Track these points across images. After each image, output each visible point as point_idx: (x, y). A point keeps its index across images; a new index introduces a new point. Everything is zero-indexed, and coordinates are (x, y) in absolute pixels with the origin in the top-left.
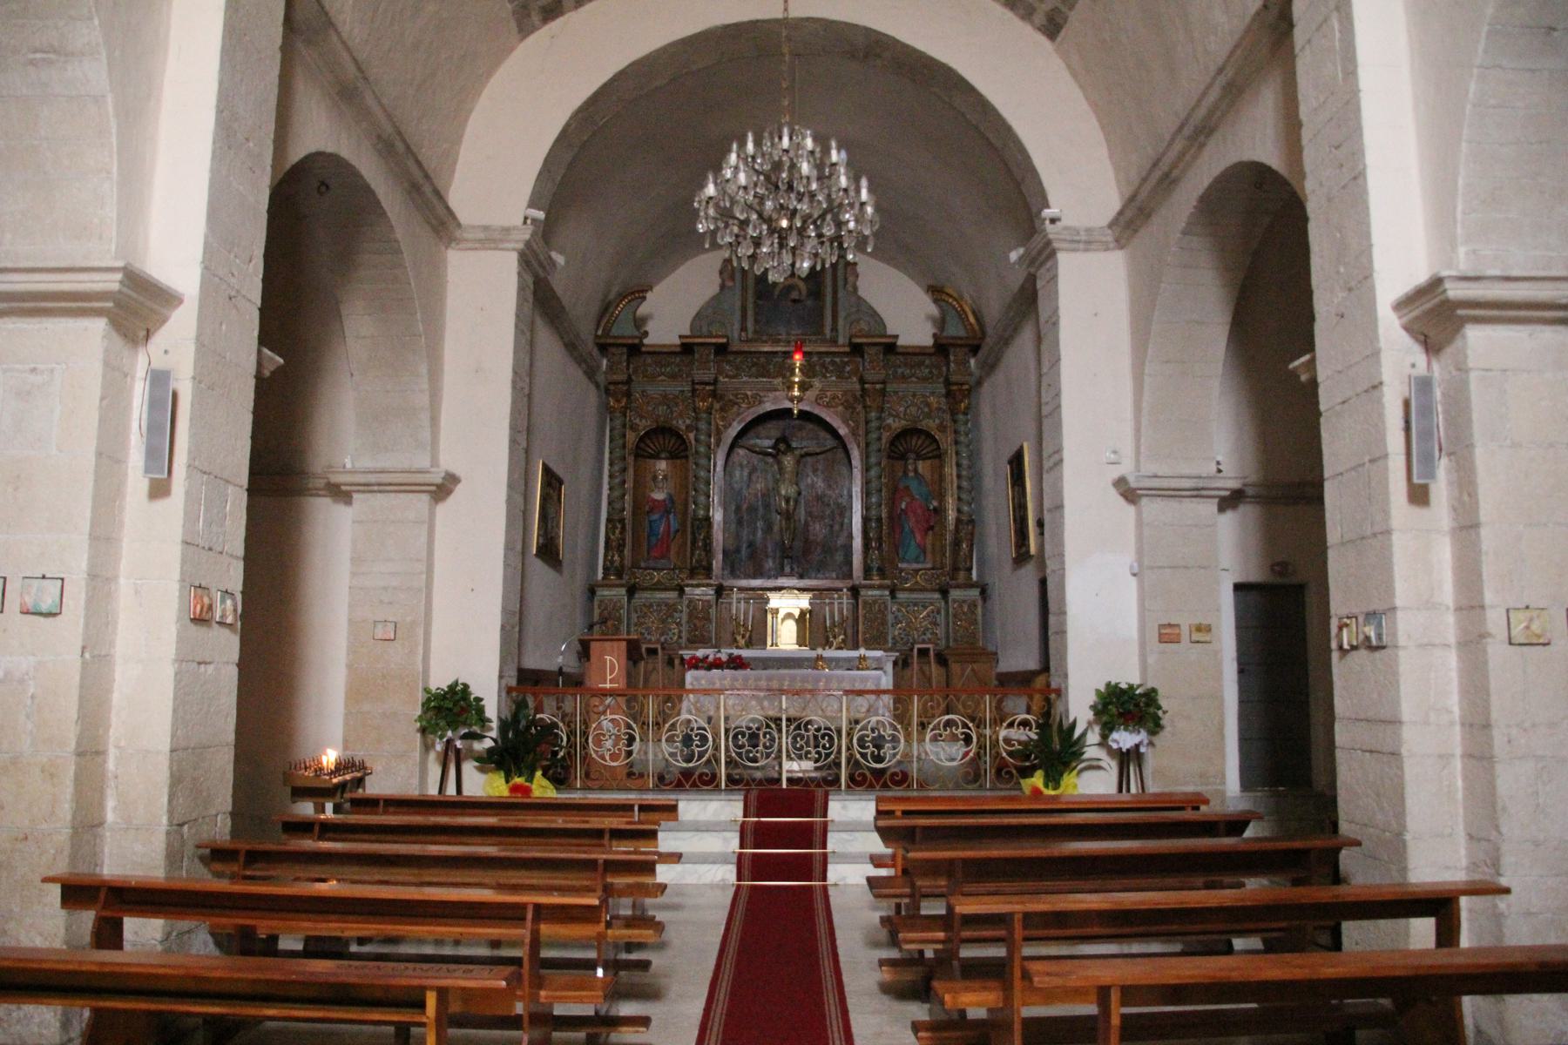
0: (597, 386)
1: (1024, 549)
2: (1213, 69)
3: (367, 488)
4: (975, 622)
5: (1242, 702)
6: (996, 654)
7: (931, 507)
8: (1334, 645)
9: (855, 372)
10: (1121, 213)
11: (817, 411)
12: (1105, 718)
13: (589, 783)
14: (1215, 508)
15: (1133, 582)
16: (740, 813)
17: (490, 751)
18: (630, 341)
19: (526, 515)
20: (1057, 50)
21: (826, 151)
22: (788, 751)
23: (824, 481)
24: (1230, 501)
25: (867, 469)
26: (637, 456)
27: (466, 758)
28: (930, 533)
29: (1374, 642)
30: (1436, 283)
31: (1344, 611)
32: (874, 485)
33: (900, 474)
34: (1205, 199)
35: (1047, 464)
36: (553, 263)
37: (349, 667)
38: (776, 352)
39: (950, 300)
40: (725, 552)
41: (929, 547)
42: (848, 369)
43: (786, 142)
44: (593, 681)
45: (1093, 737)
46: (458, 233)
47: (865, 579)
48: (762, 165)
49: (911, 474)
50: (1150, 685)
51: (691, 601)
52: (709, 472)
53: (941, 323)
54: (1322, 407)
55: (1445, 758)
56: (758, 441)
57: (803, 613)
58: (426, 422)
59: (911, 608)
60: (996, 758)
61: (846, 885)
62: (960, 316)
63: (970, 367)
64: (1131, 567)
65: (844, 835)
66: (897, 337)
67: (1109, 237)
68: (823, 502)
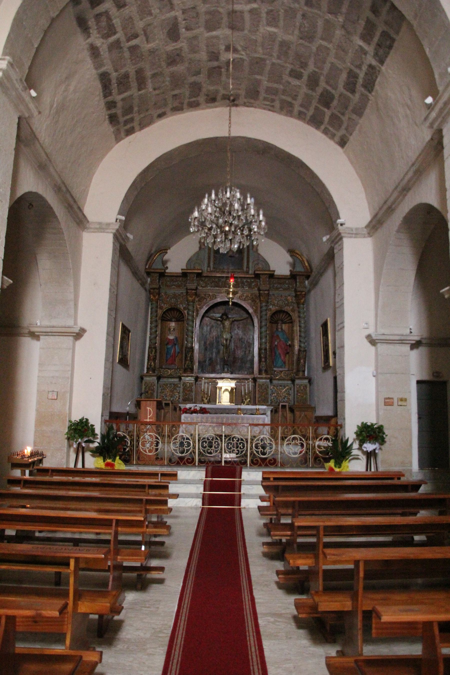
0: (146, 290)
1: (327, 364)
2: (410, 164)
3: (47, 334)
4: (306, 394)
5: (419, 431)
6: (315, 408)
7: (288, 344)
9: (256, 285)
10: (371, 222)
11: (239, 302)
12: (361, 438)
13: (139, 462)
14: (409, 348)
15: (374, 379)
16: (204, 476)
17: (97, 448)
18: (160, 271)
19: (114, 346)
20: (344, 152)
21: (245, 198)
22: (225, 449)
23: (242, 332)
24: (416, 345)
25: (260, 327)
26: (162, 320)
27: (86, 451)
28: (287, 355)
32: (263, 334)
33: (275, 330)
34: (405, 218)
35: (337, 328)
36: (128, 238)
37: (37, 410)
38: (223, 277)
39: (298, 256)
40: (199, 362)
41: (287, 362)
42: (253, 284)
43: (228, 195)
44: (142, 418)
45: (356, 446)
46: (87, 226)
47: (259, 375)
48: (218, 204)
49: (280, 330)
50: (380, 423)
51: (184, 383)
52: (193, 327)
53: (293, 265)
56: (214, 315)
57: (232, 389)
58: (73, 306)
59: (278, 387)
60: (314, 454)
61: (249, 508)
62: (302, 263)
63: (305, 284)
64: (373, 373)
65: (249, 487)
66: (274, 271)
67: (365, 231)
68: (242, 342)
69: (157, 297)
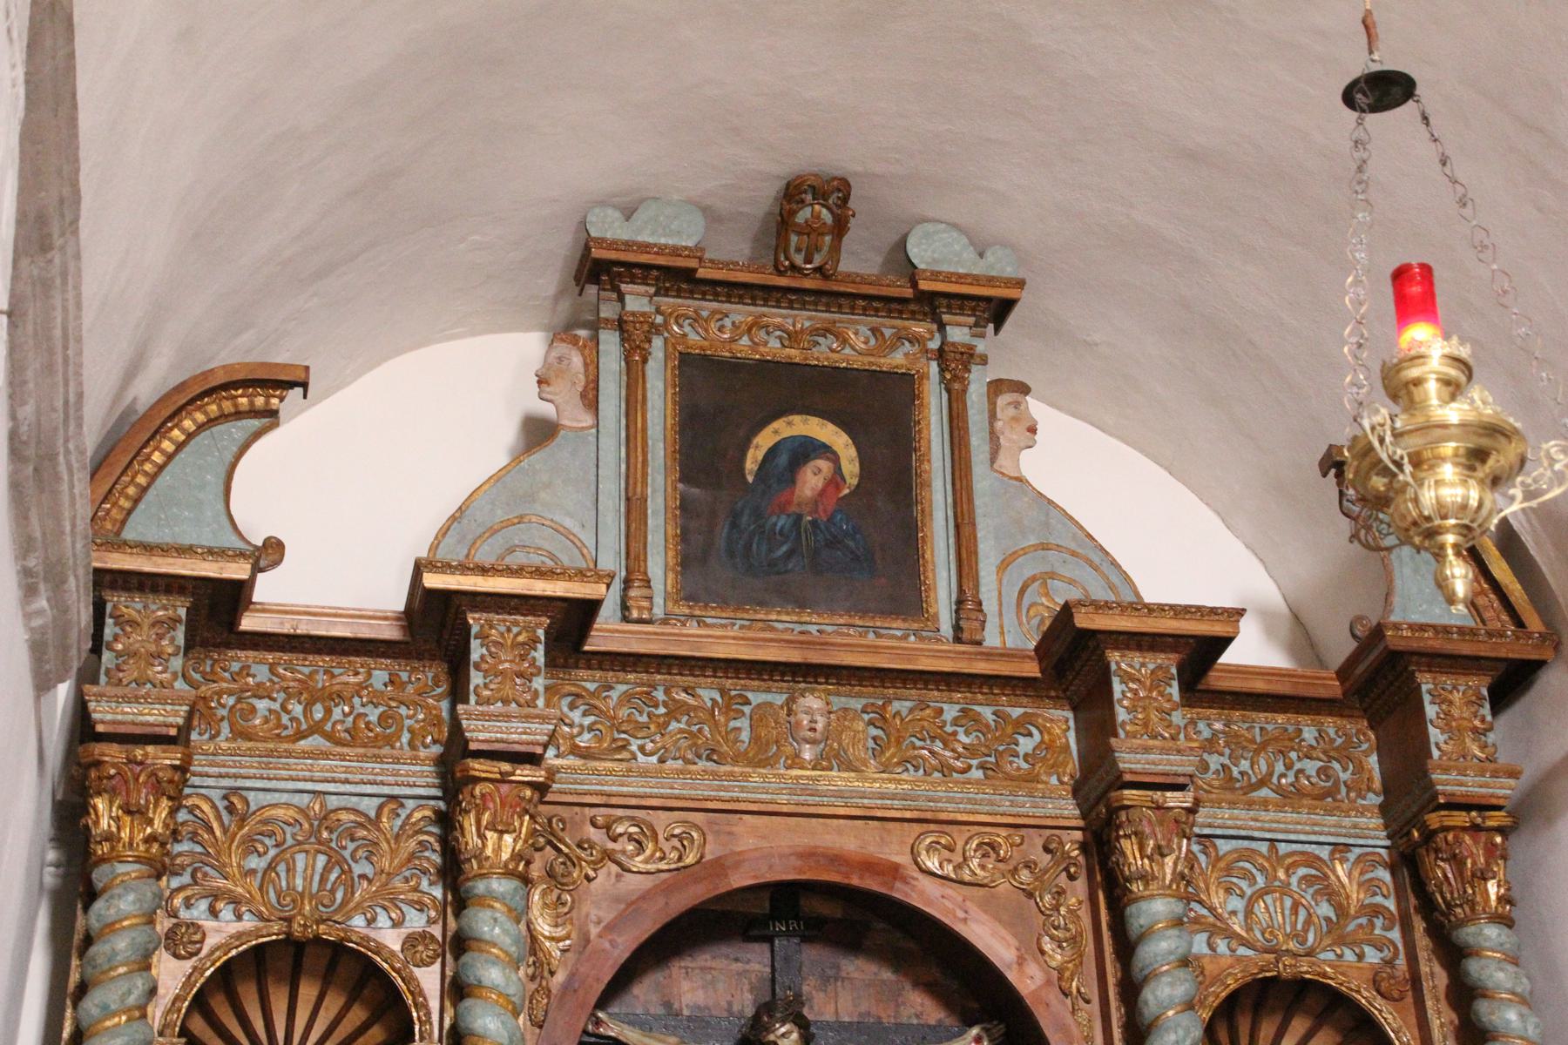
42: (1026, 745)
69: (160, 816)
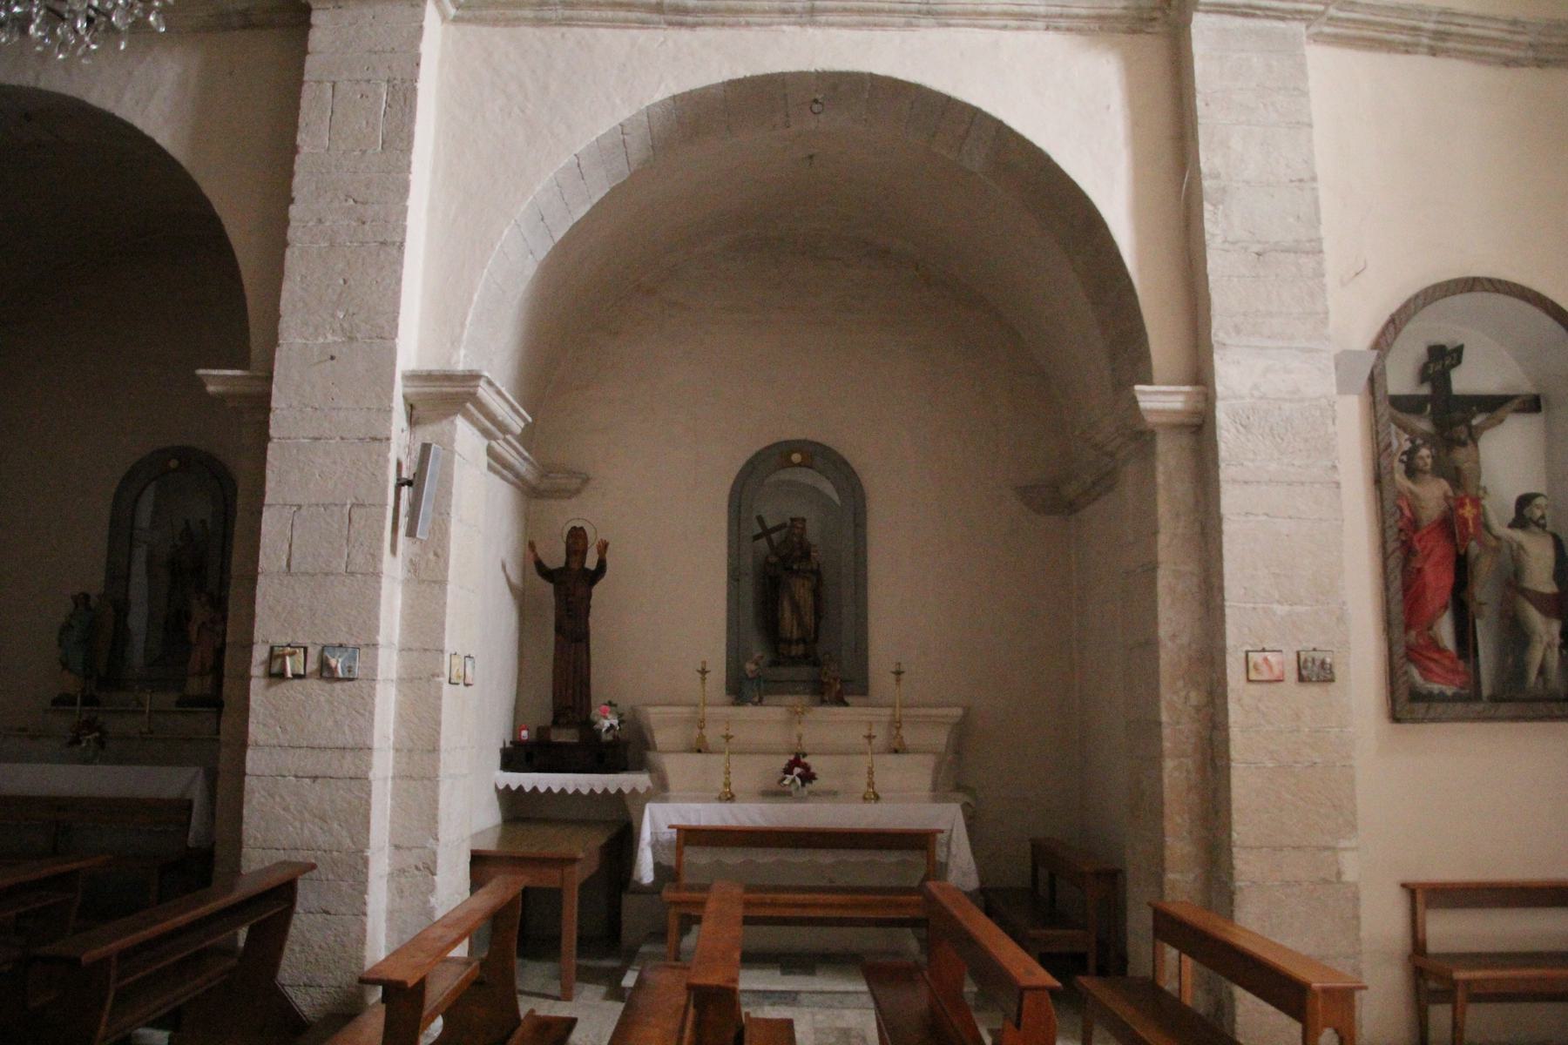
8: (257, 670)
29: (340, 674)
30: (474, 377)
31: (281, 640)
54: (272, 432)
55: (385, 779)
